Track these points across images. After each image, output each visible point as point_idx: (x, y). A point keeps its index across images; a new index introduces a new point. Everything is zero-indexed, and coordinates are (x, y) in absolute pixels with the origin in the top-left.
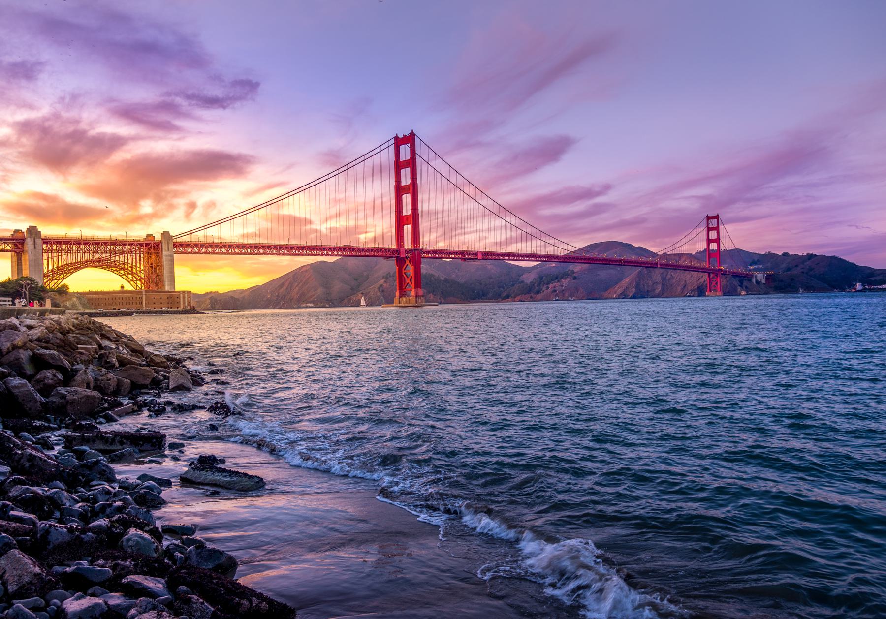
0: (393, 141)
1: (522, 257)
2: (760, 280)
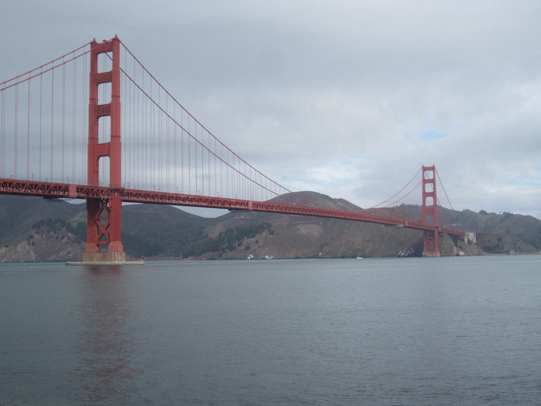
0: (89, 48)
2: (471, 240)
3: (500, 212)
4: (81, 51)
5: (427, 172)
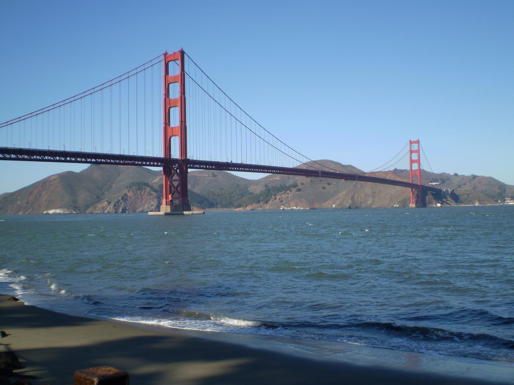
0: (162, 57)
3: (469, 175)
5: (413, 144)
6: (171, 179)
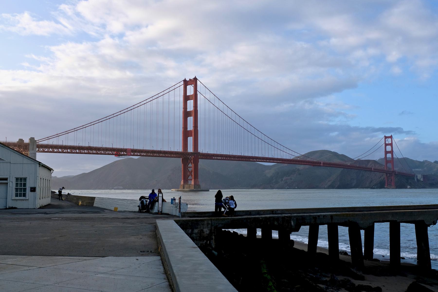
0: (182, 83)
1: (265, 160)
2: (419, 179)
4: (178, 85)
5: (387, 139)
6: (188, 166)
